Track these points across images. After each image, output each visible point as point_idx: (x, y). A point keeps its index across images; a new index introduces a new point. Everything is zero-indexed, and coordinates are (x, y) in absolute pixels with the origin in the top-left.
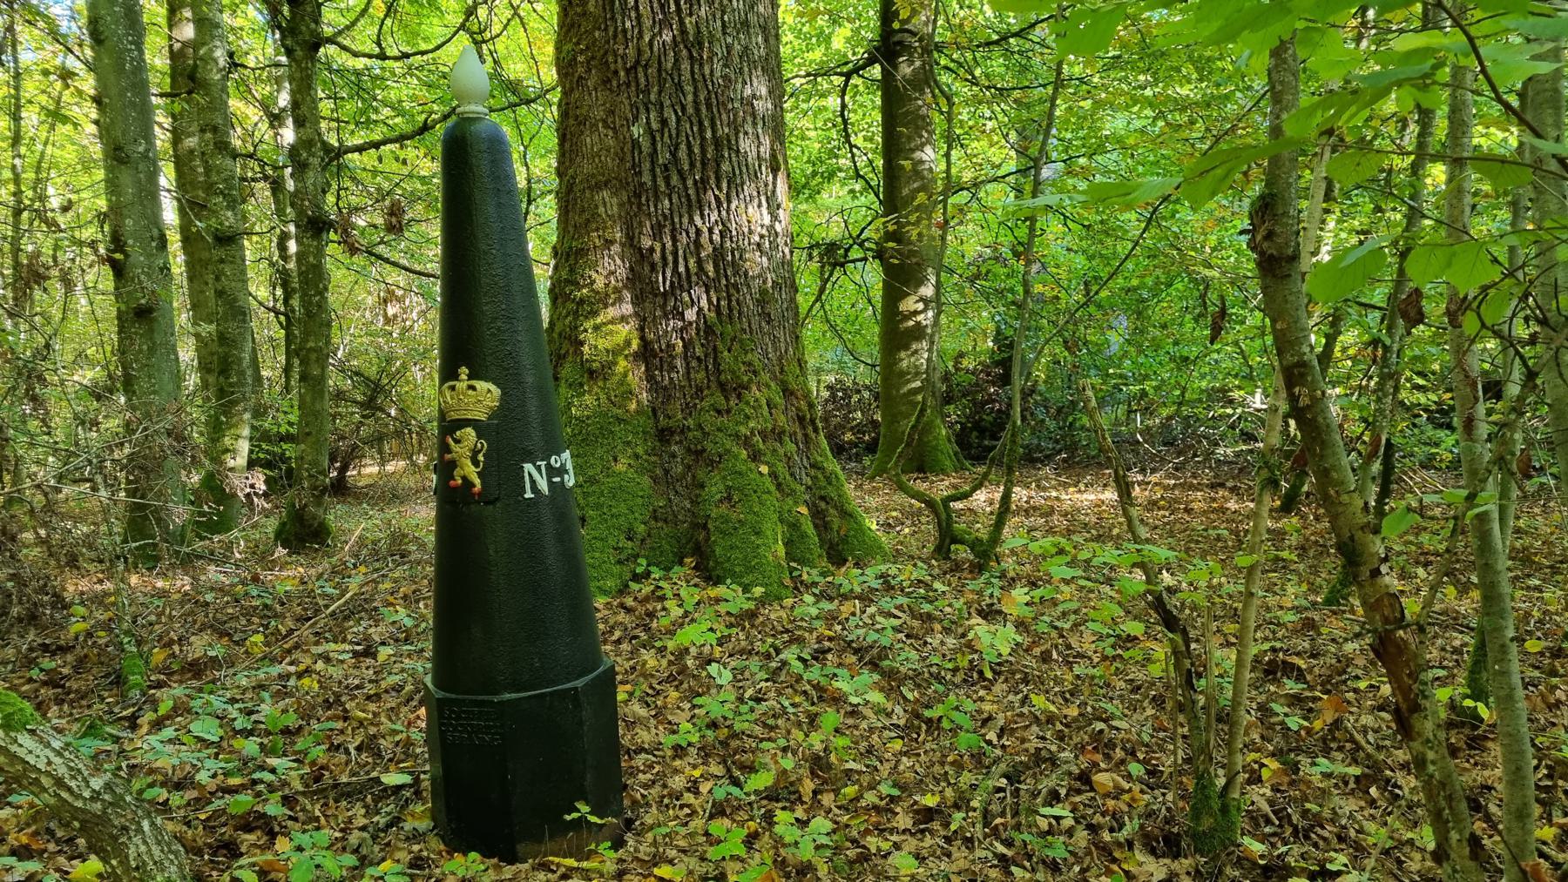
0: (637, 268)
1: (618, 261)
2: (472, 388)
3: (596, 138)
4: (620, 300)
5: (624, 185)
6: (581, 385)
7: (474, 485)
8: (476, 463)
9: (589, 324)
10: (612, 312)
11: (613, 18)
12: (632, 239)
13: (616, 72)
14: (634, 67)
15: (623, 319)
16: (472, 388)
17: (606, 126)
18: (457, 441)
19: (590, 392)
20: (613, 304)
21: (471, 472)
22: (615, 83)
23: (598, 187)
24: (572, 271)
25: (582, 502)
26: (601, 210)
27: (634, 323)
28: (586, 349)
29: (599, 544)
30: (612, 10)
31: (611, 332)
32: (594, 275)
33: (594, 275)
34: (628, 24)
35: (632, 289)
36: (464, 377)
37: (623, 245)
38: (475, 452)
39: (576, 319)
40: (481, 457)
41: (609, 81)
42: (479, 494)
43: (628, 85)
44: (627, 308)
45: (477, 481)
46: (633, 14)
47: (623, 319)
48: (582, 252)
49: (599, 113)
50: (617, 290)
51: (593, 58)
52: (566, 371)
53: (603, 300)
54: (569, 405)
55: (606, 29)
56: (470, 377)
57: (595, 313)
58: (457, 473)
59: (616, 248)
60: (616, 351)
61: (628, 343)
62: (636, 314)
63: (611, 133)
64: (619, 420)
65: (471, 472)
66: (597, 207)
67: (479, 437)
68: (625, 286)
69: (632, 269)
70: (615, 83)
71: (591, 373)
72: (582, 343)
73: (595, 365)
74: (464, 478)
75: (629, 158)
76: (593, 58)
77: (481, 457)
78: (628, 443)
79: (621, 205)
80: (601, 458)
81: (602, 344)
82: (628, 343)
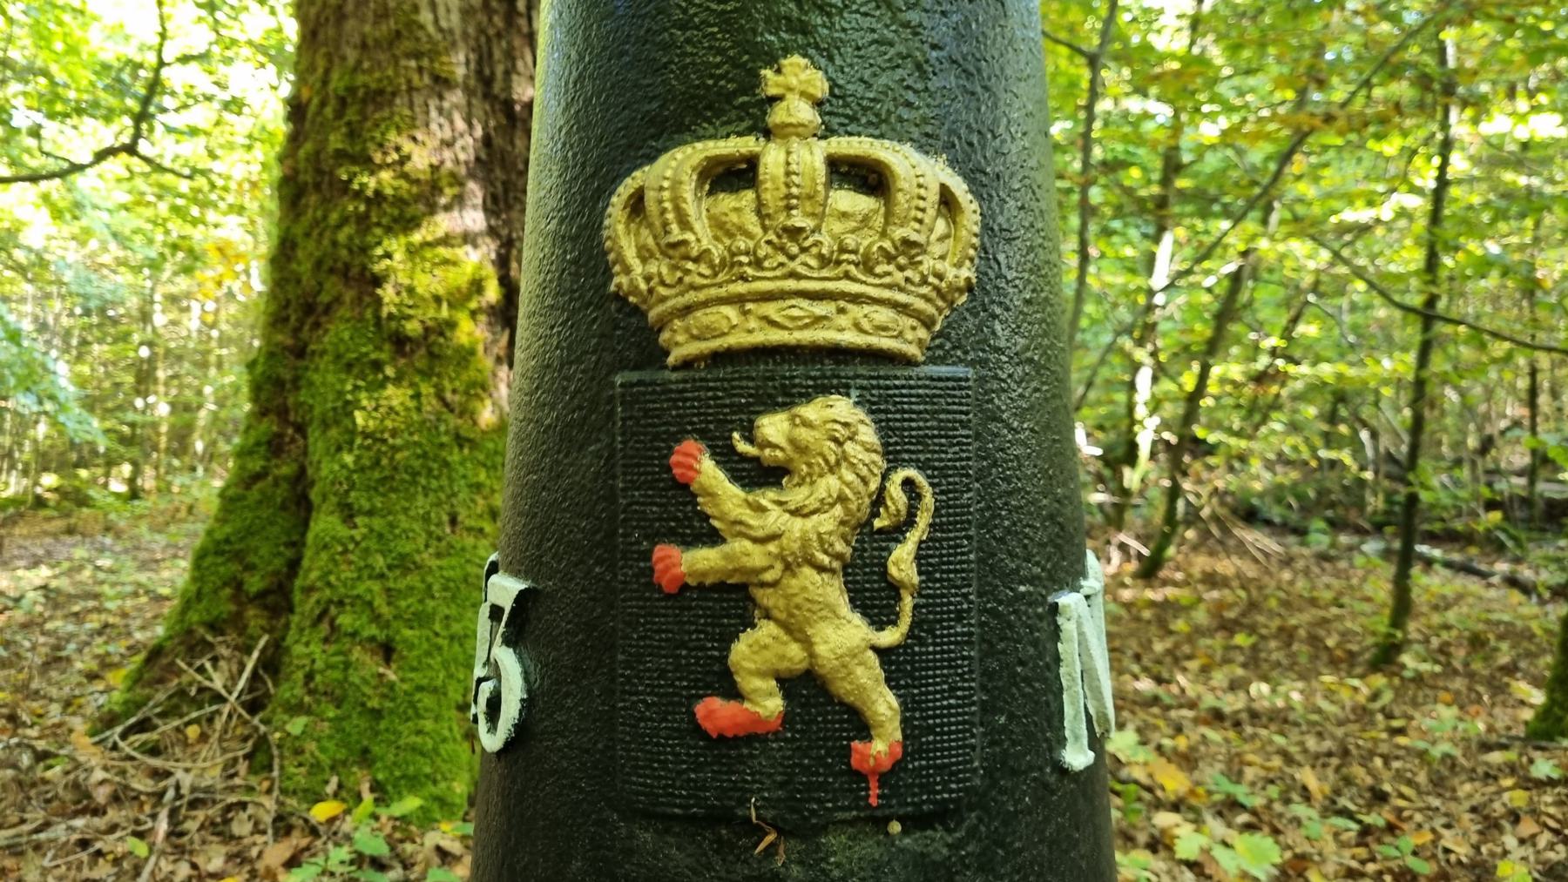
0: (498, 141)
1: (460, 125)
2: (867, 177)
4: (459, 201)
6: (377, 366)
7: (862, 727)
8: (872, 595)
10: (444, 223)
12: (487, 82)
15: (468, 238)
16: (867, 177)
18: (760, 474)
19: (397, 381)
21: (845, 639)
24: (353, 134)
25: (385, 610)
26: (425, 17)
27: (489, 248)
28: (388, 293)
29: (427, 700)
31: (446, 262)
32: (407, 147)
33: (407, 147)
35: (487, 182)
37: (469, 92)
40: (902, 561)
42: (890, 777)
44: (474, 219)
45: (884, 705)
47: (468, 238)
48: (379, 98)
50: (456, 180)
52: (338, 333)
53: (428, 194)
54: (348, 408)
56: (837, 112)
57: (410, 224)
58: (755, 652)
59: (456, 97)
60: (458, 299)
61: (477, 286)
62: (492, 232)
64: (460, 440)
65: (845, 639)
67: (893, 457)
68: (471, 175)
69: (487, 141)
71: (400, 342)
72: (378, 281)
73: (412, 328)
74: (806, 688)
77: (902, 561)
78: (478, 487)
80: (426, 519)
81: (427, 283)
82: (477, 286)
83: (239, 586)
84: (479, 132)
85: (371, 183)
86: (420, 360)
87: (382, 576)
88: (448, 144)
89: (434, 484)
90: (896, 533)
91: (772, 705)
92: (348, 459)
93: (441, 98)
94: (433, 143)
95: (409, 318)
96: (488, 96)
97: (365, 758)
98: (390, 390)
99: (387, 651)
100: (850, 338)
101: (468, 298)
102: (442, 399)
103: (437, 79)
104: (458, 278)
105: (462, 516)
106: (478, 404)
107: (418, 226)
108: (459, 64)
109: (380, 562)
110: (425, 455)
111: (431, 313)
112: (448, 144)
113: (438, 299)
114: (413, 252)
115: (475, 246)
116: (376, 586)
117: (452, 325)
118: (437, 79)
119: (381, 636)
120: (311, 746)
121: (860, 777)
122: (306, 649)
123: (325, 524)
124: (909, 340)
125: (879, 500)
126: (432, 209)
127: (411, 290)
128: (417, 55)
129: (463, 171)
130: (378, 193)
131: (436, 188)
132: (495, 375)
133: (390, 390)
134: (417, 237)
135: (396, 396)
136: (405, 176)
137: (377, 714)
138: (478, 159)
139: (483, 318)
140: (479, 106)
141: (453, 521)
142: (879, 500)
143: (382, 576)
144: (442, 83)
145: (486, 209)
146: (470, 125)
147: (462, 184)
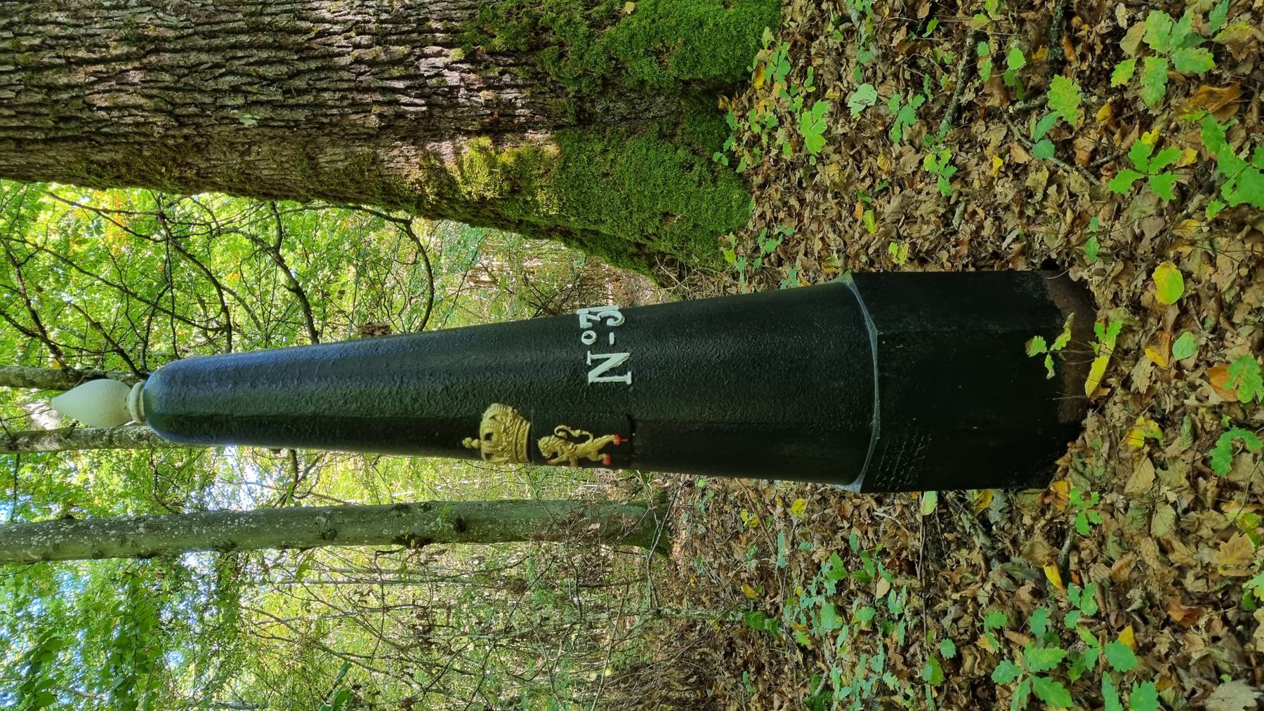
0: (402, 133)
1: (396, 152)
2: (488, 437)
3: (262, 165)
4: (437, 155)
5: (310, 139)
6: (526, 202)
7: (611, 443)
8: (583, 439)
9: (464, 189)
10: (450, 164)
11: (125, 135)
12: (370, 136)
13: (186, 137)
14: (177, 118)
15: (457, 152)
17: (248, 152)
19: (533, 195)
20: (442, 162)
22: (199, 140)
23: (315, 167)
26: (340, 165)
27: (461, 140)
28: (489, 195)
29: (693, 202)
30: (116, 136)
31: (471, 166)
34: (129, 120)
35: (426, 140)
36: (475, 443)
37: (377, 146)
38: (569, 438)
39: (457, 201)
40: (577, 433)
41: (196, 145)
42: (621, 437)
43: (198, 126)
44: (446, 147)
45: (606, 439)
46: (115, 113)
47: (457, 152)
49: (235, 159)
50: (426, 156)
51: (174, 160)
54: (546, 216)
55: (140, 144)
56: (475, 435)
57: (452, 181)
59: (381, 152)
60: (491, 163)
61: (482, 150)
62: (452, 138)
63: (255, 148)
64: (564, 168)
66: (337, 170)
67: (551, 433)
68: (423, 147)
69: (403, 139)
70: (199, 140)
71: (513, 191)
72: (483, 198)
73: (506, 187)
74: (600, 452)
75: (280, 132)
76: (174, 160)
77: (577, 433)
78: (590, 160)
79: (334, 144)
80: (604, 190)
81: (483, 178)
82: (482, 150)
83: (633, 254)
84: (399, 143)
85: (431, 197)
86: (524, 184)
87: (631, 213)
88: (407, 159)
89: (587, 184)
90: (568, 434)
91: (604, 456)
92: (572, 219)
93: (383, 161)
94: (407, 168)
95: (501, 188)
96: (378, 137)
97: (714, 233)
98: (538, 198)
99: (666, 215)
100: (525, 441)
101: (489, 155)
102: (542, 176)
103: (373, 163)
104: (479, 159)
105: (603, 170)
106: (546, 156)
107: (453, 178)
108: (364, 150)
109: (624, 213)
110: (572, 186)
111: (498, 176)
112: (407, 159)
113: (491, 173)
114: (467, 182)
115: (461, 148)
116: (635, 216)
117: (504, 166)
118: (373, 163)
119: (660, 217)
120: (705, 256)
121: (621, 443)
122: (664, 246)
123: (604, 230)
124: (527, 426)
125: (561, 438)
126: (444, 170)
127: (487, 185)
128: (362, 172)
129: (420, 152)
130: (436, 195)
131: (432, 168)
132: (531, 141)
133: (538, 198)
134: (459, 179)
135: (541, 197)
136: (427, 182)
137: (695, 226)
138: (413, 144)
139: (500, 149)
140: (384, 141)
141: (606, 175)
142: (561, 438)
143: (631, 213)
144: (375, 160)
145: (440, 141)
146: (395, 147)
147: (428, 154)
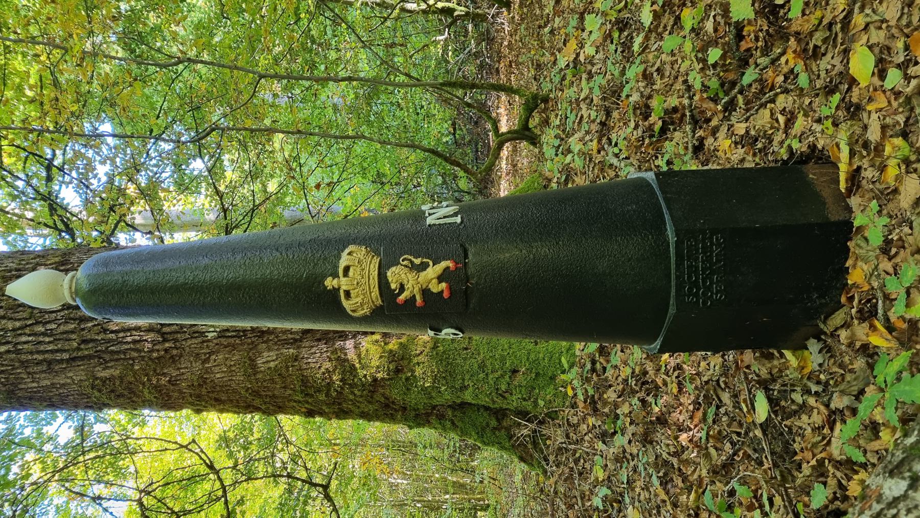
2: (347, 269)
3: (216, 369)
4: (343, 349)
5: (254, 346)
6: (407, 379)
7: (448, 268)
8: (423, 267)
9: (361, 373)
10: (351, 355)
11: (124, 352)
12: (296, 340)
13: (166, 350)
14: (163, 334)
15: (356, 347)
16: (347, 269)
17: (207, 360)
18: (402, 288)
19: (413, 371)
20: (346, 354)
21: (433, 271)
22: (175, 352)
23: (254, 366)
24: (319, 391)
25: (499, 373)
26: (272, 365)
28: (379, 376)
29: (532, 356)
30: (118, 352)
32: (323, 370)
33: (323, 370)
34: (129, 339)
36: (335, 282)
37: (299, 347)
38: (414, 268)
39: (356, 385)
40: (417, 261)
41: (172, 357)
43: (176, 340)
44: (349, 344)
45: (444, 264)
46: (121, 335)
48: (304, 381)
49: (197, 365)
50: (335, 351)
51: (155, 370)
52: (395, 394)
53: (342, 362)
54: (424, 389)
55: (133, 359)
56: (335, 275)
58: (435, 288)
59: (304, 353)
63: (213, 357)
65: (433, 271)
66: (269, 368)
67: (398, 263)
70: (175, 352)
71: (398, 371)
72: (375, 380)
74: (440, 279)
75: (232, 340)
76: (155, 370)
77: (417, 261)
79: (269, 350)
83: (495, 428)
87: (487, 374)
89: (452, 356)
91: (444, 285)
92: (443, 388)
97: (553, 378)
99: (515, 372)
100: (376, 272)
103: (296, 360)
109: (482, 375)
110: (441, 360)
119: (509, 374)
122: (514, 401)
123: (468, 396)
124: (376, 260)
125: (406, 266)
127: (378, 367)
128: (287, 367)
134: (358, 366)
136: (334, 370)
137: (537, 374)
141: (466, 349)
142: (406, 266)
145: (345, 340)
